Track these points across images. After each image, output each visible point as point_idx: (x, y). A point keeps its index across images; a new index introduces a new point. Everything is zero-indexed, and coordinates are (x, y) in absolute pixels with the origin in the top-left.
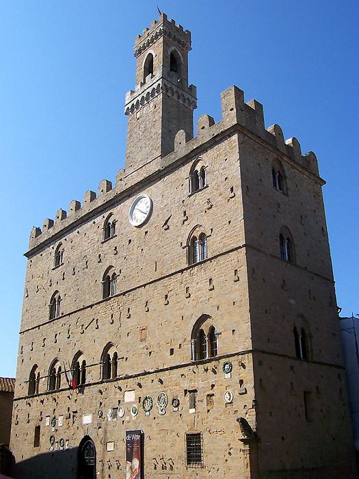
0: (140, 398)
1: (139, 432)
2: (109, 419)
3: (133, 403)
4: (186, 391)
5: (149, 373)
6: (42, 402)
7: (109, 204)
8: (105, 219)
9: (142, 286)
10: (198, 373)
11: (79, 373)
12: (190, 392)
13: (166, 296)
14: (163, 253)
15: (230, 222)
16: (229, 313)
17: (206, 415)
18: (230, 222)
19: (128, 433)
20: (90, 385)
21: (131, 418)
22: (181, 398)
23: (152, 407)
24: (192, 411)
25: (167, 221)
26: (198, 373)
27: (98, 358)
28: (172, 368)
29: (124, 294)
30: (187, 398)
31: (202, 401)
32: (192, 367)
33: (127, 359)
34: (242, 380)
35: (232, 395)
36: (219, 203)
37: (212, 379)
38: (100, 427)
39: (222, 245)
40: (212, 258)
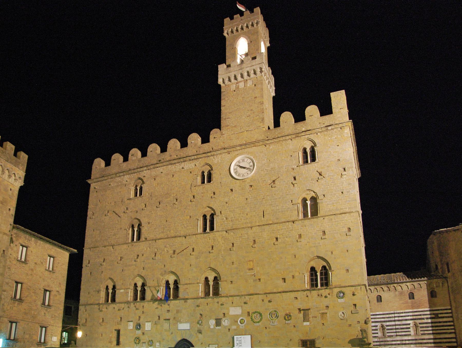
0: (249, 312)
2: (212, 327)
4: (299, 309)
5: (258, 294)
9: (249, 227)
10: (312, 297)
11: (173, 291)
12: (303, 310)
14: (271, 205)
20: (186, 300)
23: (261, 320)
24: (305, 323)
26: (312, 297)
28: (284, 292)
30: (301, 315)
31: (316, 317)
37: (326, 302)
38: (200, 333)
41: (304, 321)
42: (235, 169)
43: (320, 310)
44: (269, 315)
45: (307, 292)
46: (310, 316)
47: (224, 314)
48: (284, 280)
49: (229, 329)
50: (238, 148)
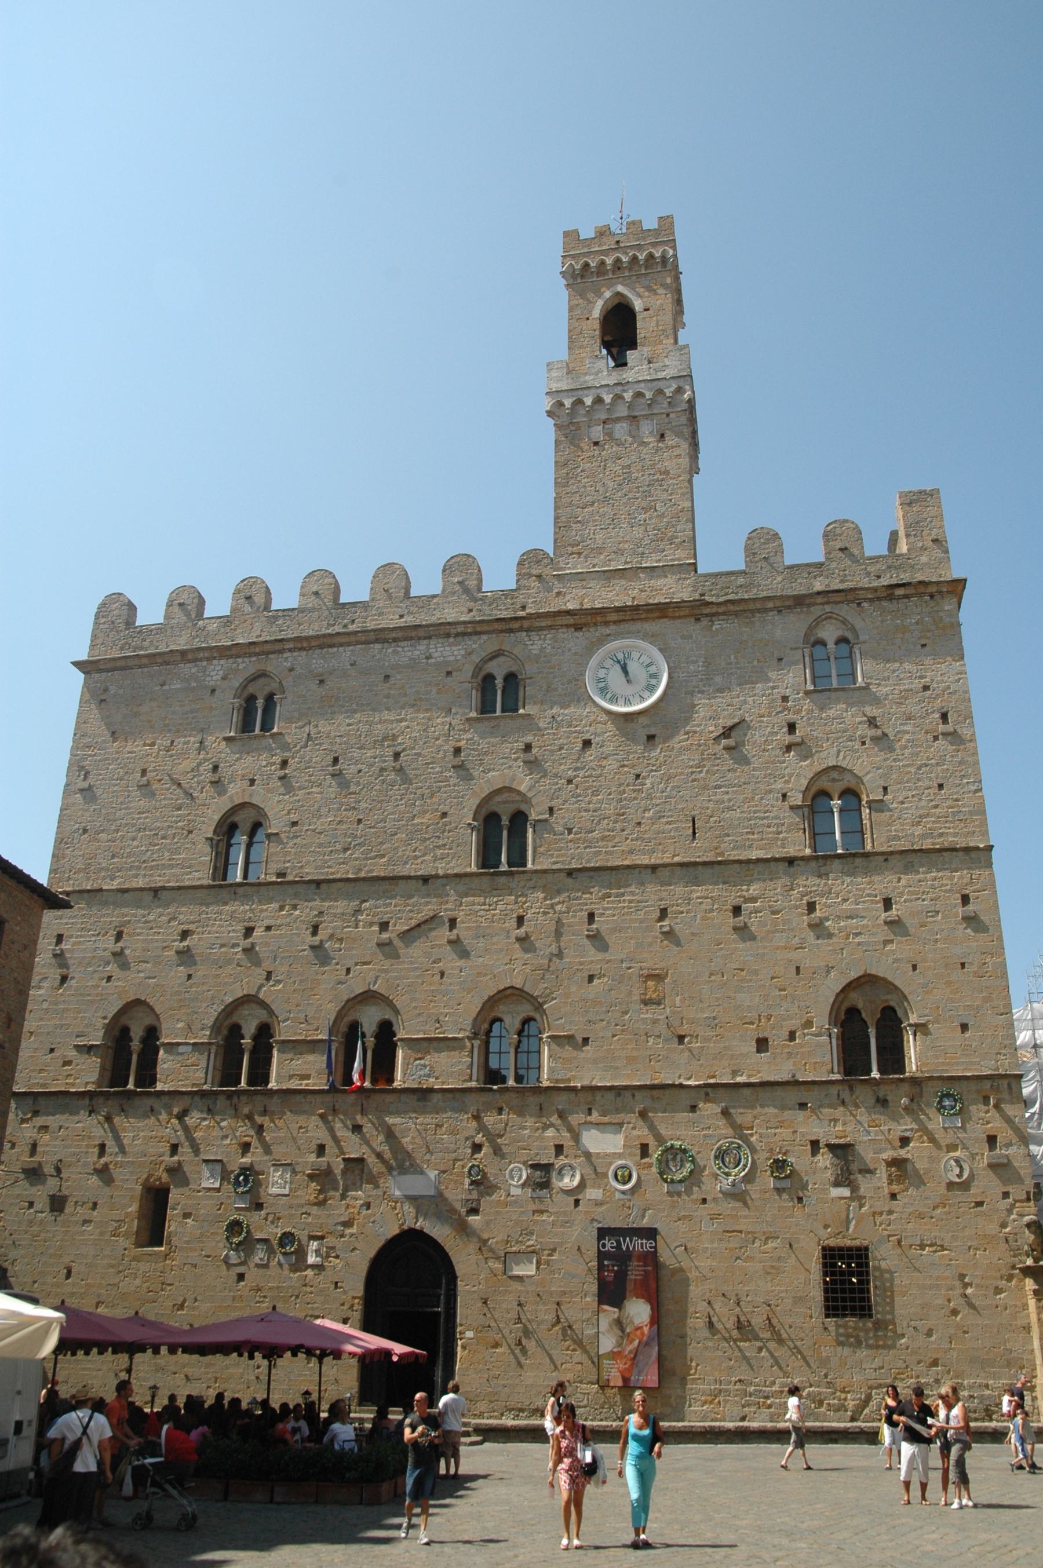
1: (651, 1233)
2: (514, 1191)
3: (620, 1156)
4: (815, 1145)
6: (181, 1116)
7: (496, 626)
8: (476, 659)
9: (646, 867)
12: (828, 1146)
13: (737, 910)
15: (941, 786)
16: (949, 984)
17: (886, 1205)
18: (941, 786)
19: (603, 1233)
21: (609, 1191)
22: (799, 1159)
25: (727, 732)
27: (459, 1023)
29: (570, 873)
32: (834, 1090)
33: (586, 1041)
34: (995, 1137)
35: (966, 1167)
36: (907, 737)
39: (919, 830)
40: (892, 853)
41: (837, 1184)
42: (599, 680)
43: (884, 1150)
44: (716, 1157)
45: (840, 1087)
46: (854, 1167)
47: (559, 1149)
48: (762, 1044)
49: (577, 1202)
50: (613, 617)
